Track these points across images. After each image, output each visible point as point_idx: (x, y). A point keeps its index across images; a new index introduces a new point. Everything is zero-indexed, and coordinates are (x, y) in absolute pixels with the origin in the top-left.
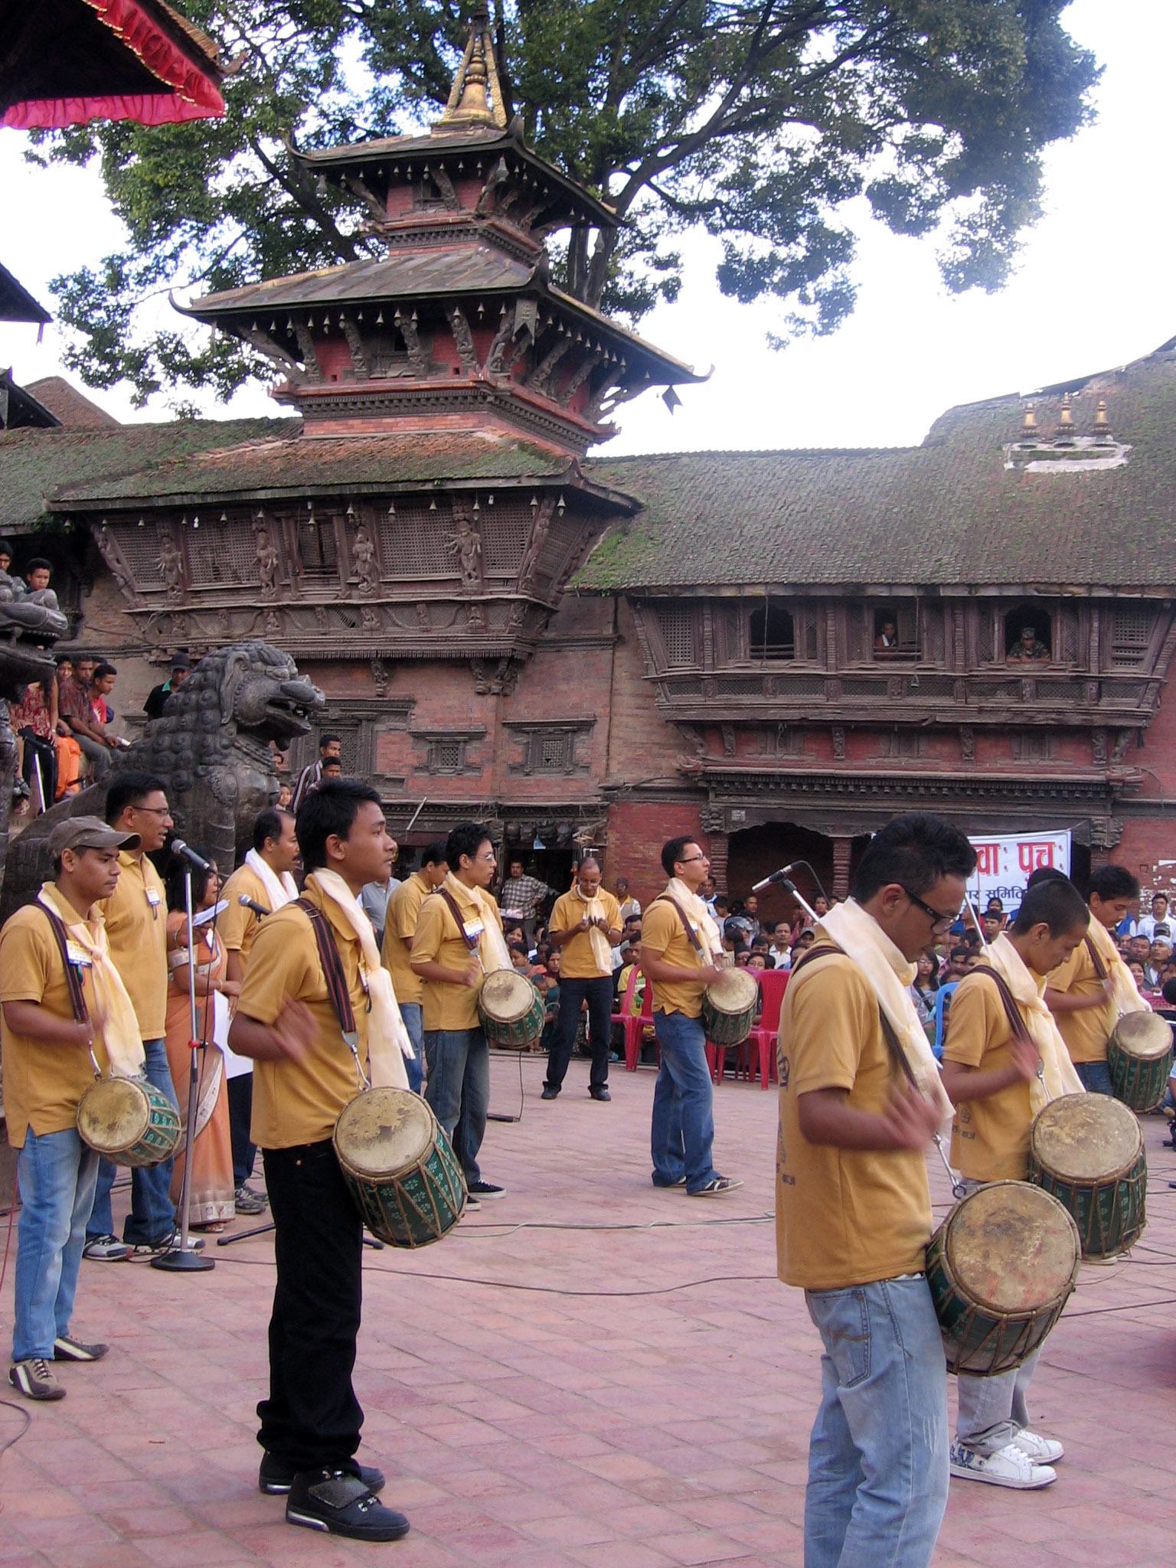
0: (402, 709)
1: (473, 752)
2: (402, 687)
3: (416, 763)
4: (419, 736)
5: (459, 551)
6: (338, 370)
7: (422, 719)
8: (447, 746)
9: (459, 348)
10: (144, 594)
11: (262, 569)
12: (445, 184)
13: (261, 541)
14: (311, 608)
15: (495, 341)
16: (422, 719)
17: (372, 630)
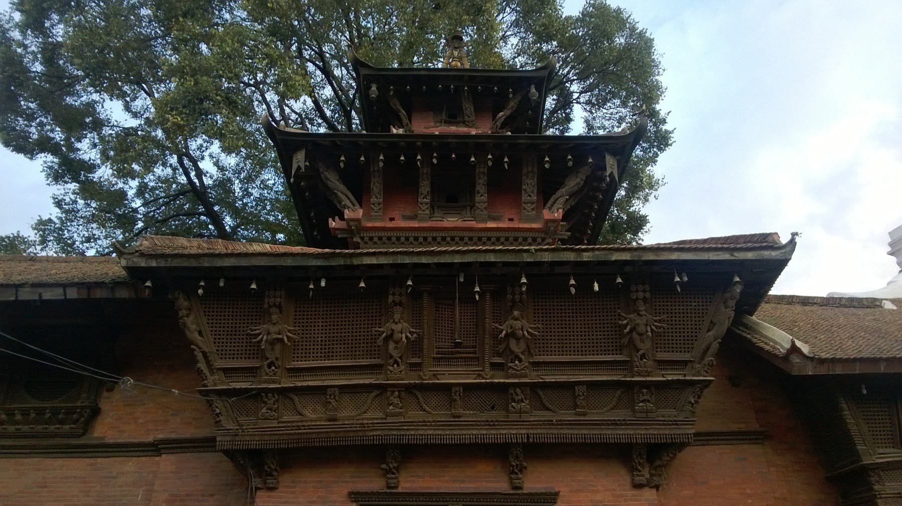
5: (631, 331)
6: (396, 214)
9: (525, 198)
10: (225, 371)
11: (391, 345)
12: (468, 108)
13: (397, 316)
14: (446, 388)
15: (558, 194)
17: (521, 412)
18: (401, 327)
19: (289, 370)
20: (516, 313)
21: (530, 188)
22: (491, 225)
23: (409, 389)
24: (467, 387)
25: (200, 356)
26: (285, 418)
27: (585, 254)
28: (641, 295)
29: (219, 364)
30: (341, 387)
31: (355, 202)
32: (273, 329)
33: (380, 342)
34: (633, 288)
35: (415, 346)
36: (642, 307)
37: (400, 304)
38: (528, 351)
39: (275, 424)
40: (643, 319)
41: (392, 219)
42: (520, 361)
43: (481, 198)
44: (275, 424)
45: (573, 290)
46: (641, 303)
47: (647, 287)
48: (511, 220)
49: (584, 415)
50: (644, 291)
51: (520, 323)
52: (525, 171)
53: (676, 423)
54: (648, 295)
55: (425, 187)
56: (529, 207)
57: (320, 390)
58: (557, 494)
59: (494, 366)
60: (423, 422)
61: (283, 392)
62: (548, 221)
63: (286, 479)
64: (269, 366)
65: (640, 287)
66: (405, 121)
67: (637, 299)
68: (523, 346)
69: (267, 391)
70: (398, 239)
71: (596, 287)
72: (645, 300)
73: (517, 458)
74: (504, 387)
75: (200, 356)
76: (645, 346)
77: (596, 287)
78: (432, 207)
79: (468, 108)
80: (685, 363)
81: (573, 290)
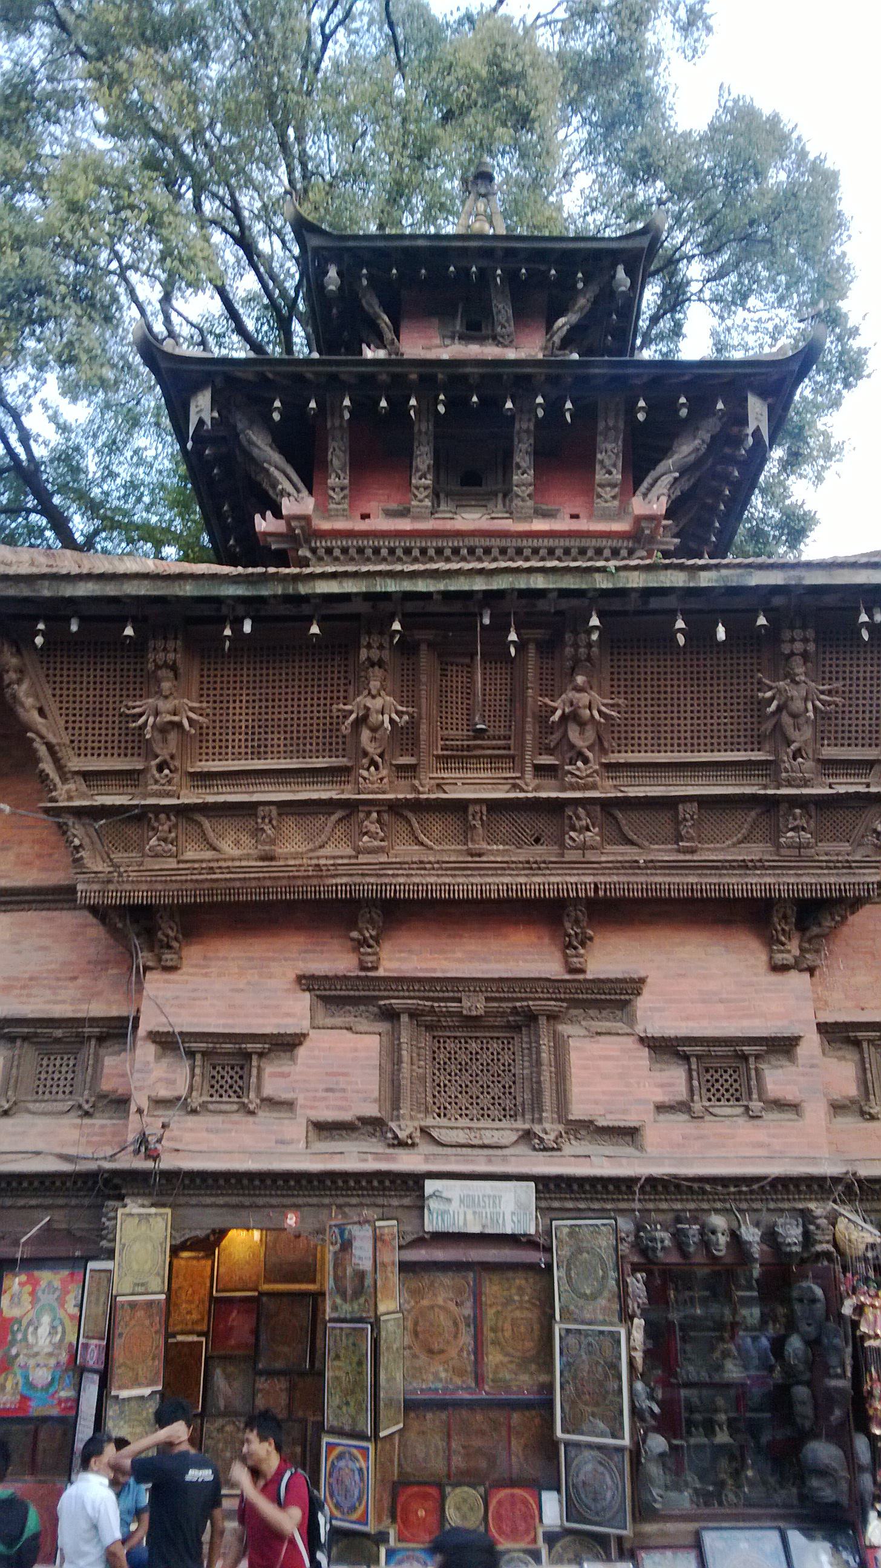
0: (616, 998)
1: (777, 1079)
2: (609, 957)
3: (660, 1097)
4: (663, 1048)
5: (780, 709)
6: (373, 506)
7: (656, 1015)
8: (724, 1068)
9: (600, 476)
10: (86, 775)
11: (366, 734)
12: (503, 309)
13: (375, 685)
14: (460, 807)
15: (661, 467)
16: (656, 1015)
17: (584, 847)
18: (382, 704)
19: (193, 775)
20: (580, 679)
21: (609, 458)
22: (540, 525)
23: (395, 808)
24: (495, 806)
25: (43, 751)
26: (189, 855)
27: (703, 574)
28: (798, 646)
29: (75, 764)
30: (280, 804)
31: (300, 485)
32: (164, 705)
33: (346, 728)
34: (787, 635)
35: (406, 736)
36: (799, 669)
37: (380, 664)
38: (599, 743)
39: (172, 863)
40: (802, 691)
41: (365, 516)
42: (586, 761)
43: (523, 478)
44: (172, 863)
45: (681, 639)
46: (798, 660)
47: (810, 633)
48: (575, 517)
49: (693, 851)
50: (805, 640)
51: (588, 697)
52: (601, 426)
53: (848, 866)
54: (811, 647)
55: (423, 459)
56: (608, 493)
57: (249, 809)
58: (642, 981)
59: (540, 770)
60: (422, 862)
61: (184, 812)
62: (638, 519)
63: (193, 953)
64: (160, 769)
65: (798, 633)
66: (389, 335)
67: (792, 654)
68: (590, 734)
69: (158, 809)
70: (376, 551)
71: (721, 633)
72: (805, 656)
73: (577, 922)
74: (556, 807)
75: (43, 751)
76: (802, 736)
77: (721, 633)
78: (436, 495)
79: (503, 309)
80: (870, 764)
81: (681, 639)
